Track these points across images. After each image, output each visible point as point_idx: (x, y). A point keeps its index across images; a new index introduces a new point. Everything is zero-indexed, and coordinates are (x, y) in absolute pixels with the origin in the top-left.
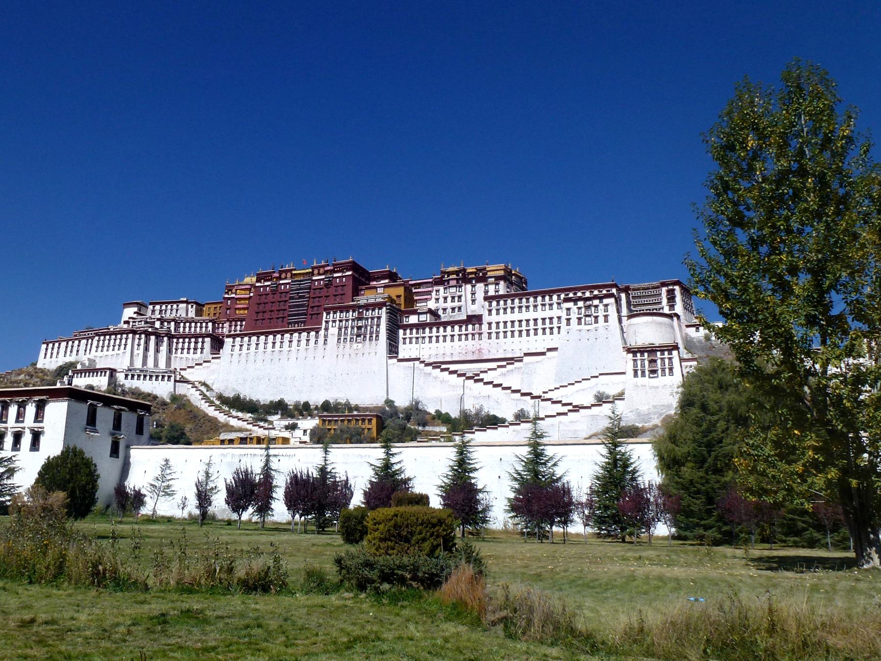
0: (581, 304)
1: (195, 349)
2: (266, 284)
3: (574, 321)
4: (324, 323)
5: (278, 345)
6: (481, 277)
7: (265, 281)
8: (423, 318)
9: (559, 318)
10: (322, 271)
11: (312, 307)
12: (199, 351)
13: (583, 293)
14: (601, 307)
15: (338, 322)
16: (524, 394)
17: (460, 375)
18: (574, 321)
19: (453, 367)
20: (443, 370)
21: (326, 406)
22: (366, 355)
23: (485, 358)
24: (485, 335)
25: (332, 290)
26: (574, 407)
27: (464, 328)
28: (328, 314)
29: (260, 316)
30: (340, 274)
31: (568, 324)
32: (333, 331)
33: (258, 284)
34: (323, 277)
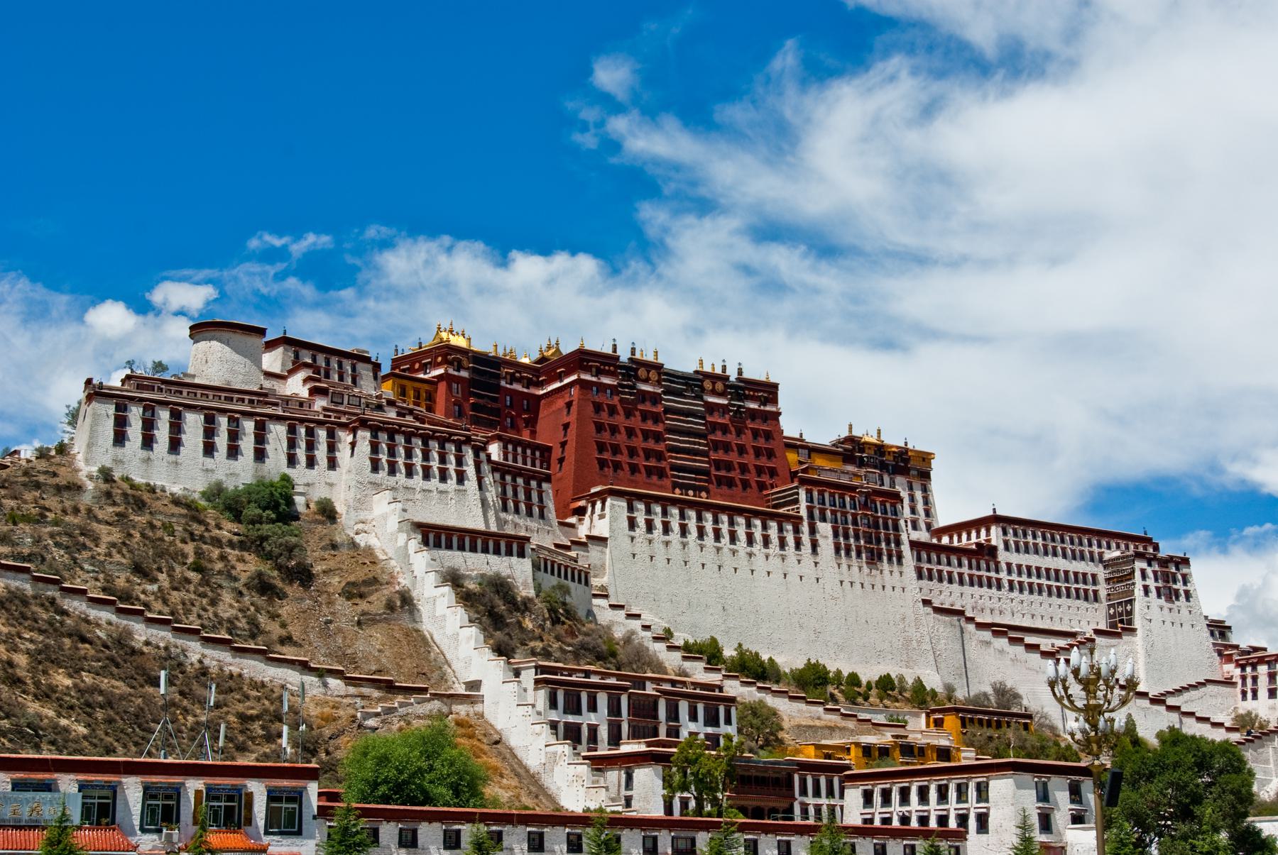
2: (606, 380)
4: (803, 513)
7: (599, 372)
9: (1094, 576)
11: (718, 464)
13: (1145, 548)
14: (1180, 577)
15: (828, 513)
17: (1046, 655)
19: (1030, 639)
20: (1013, 641)
21: (886, 684)
22: (888, 588)
25: (747, 439)
27: (974, 562)
28: (809, 492)
29: (606, 456)
32: (825, 529)
33: (587, 377)
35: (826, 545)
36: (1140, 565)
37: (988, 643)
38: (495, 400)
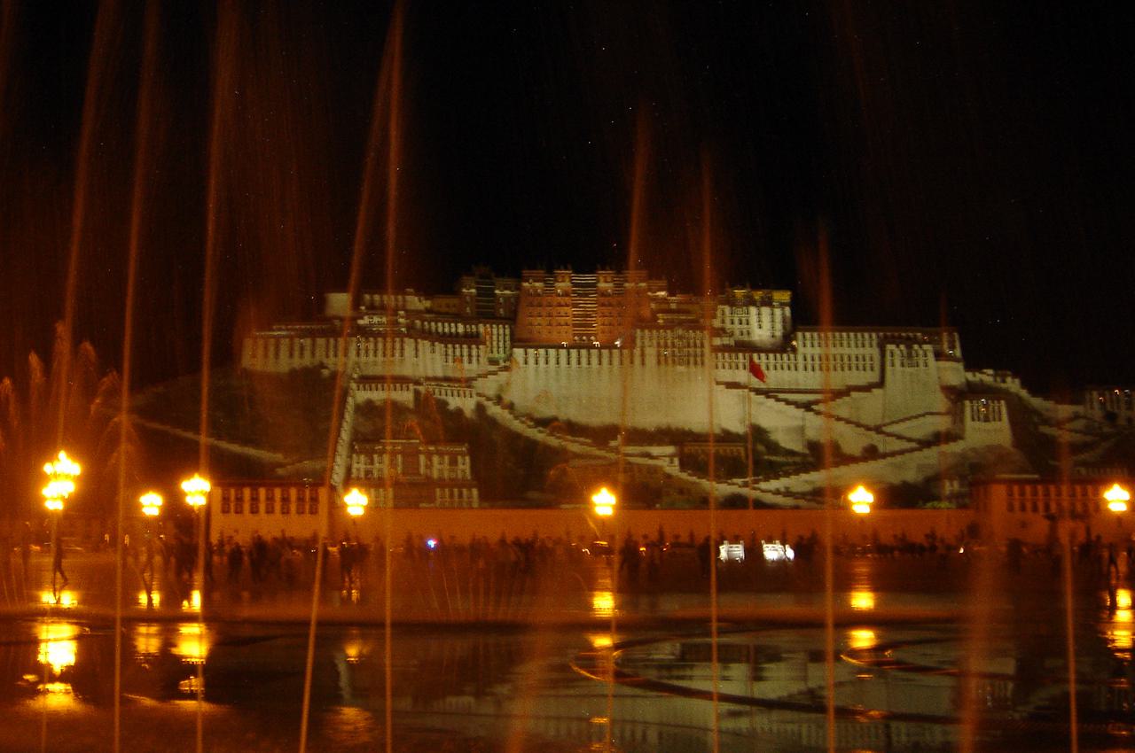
0: (902, 347)
1: (470, 356)
3: (897, 363)
5: (584, 360)
6: (768, 302)
7: (535, 281)
8: (726, 341)
9: (871, 359)
10: (609, 280)
12: (474, 359)
14: (921, 352)
16: (868, 428)
17: (797, 405)
18: (897, 363)
20: (778, 400)
23: (802, 387)
24: (801, 366)
26: (919, 442)
30: (633, 285)
31: (893, 365)
32: (651, 352)
33: (526, 284)
34: (611, 285)
35: (651, 360)
36: (890, 347)
37: (761, 404)
38: (488, 301)
